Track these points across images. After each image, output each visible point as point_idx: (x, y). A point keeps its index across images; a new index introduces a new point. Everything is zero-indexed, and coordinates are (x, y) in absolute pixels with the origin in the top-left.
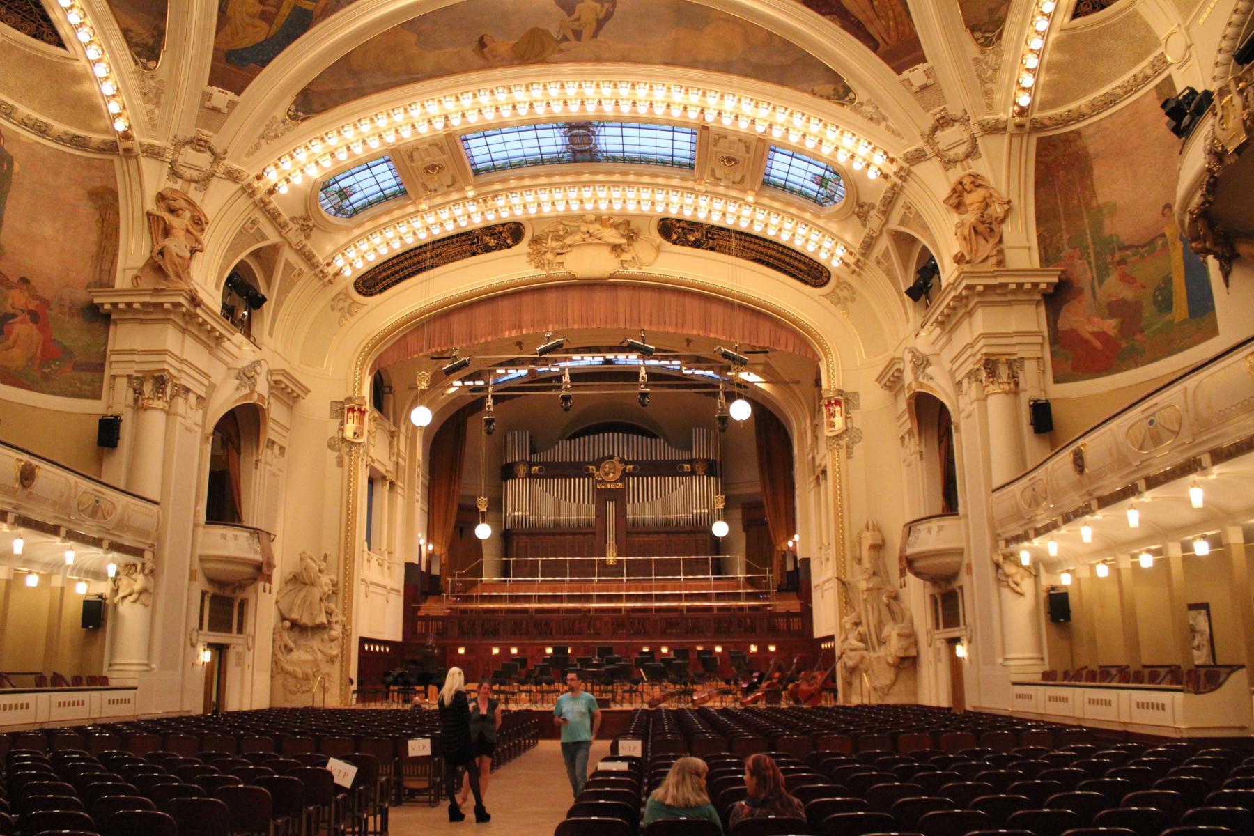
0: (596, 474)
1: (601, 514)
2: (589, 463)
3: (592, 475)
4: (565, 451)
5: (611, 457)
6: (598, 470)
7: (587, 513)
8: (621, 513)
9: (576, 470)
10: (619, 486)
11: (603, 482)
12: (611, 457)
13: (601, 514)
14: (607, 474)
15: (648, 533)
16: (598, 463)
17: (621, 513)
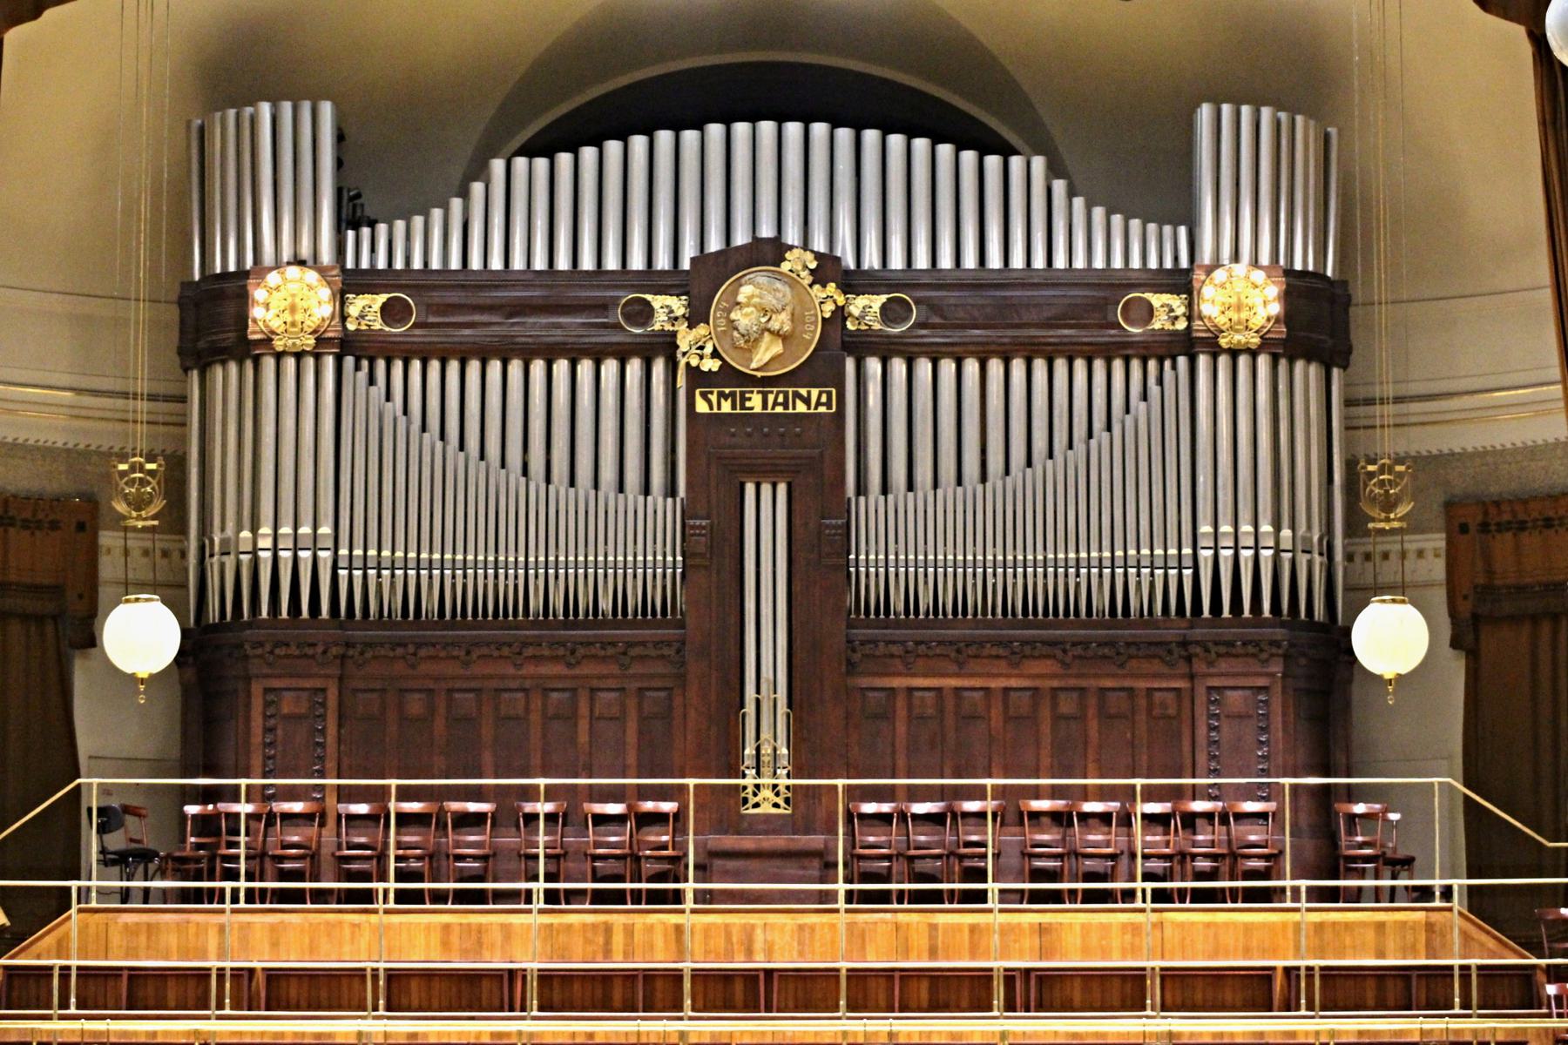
0: (686, 339)
1: (713, 549)
2: (653, 280)
3: (666, 345)
4: (515, 220)
5: (769, 252)
6: (696, 317)
7: (625, 543)
8: (821, 548)
9: (576, 316)
10: (811, 401)
11: (730, 377)
12: (769, 252)
13: (713, 549)
14: (752, 342)
15: (962, 654)
16: (703, 283)
17: (821, 548)
